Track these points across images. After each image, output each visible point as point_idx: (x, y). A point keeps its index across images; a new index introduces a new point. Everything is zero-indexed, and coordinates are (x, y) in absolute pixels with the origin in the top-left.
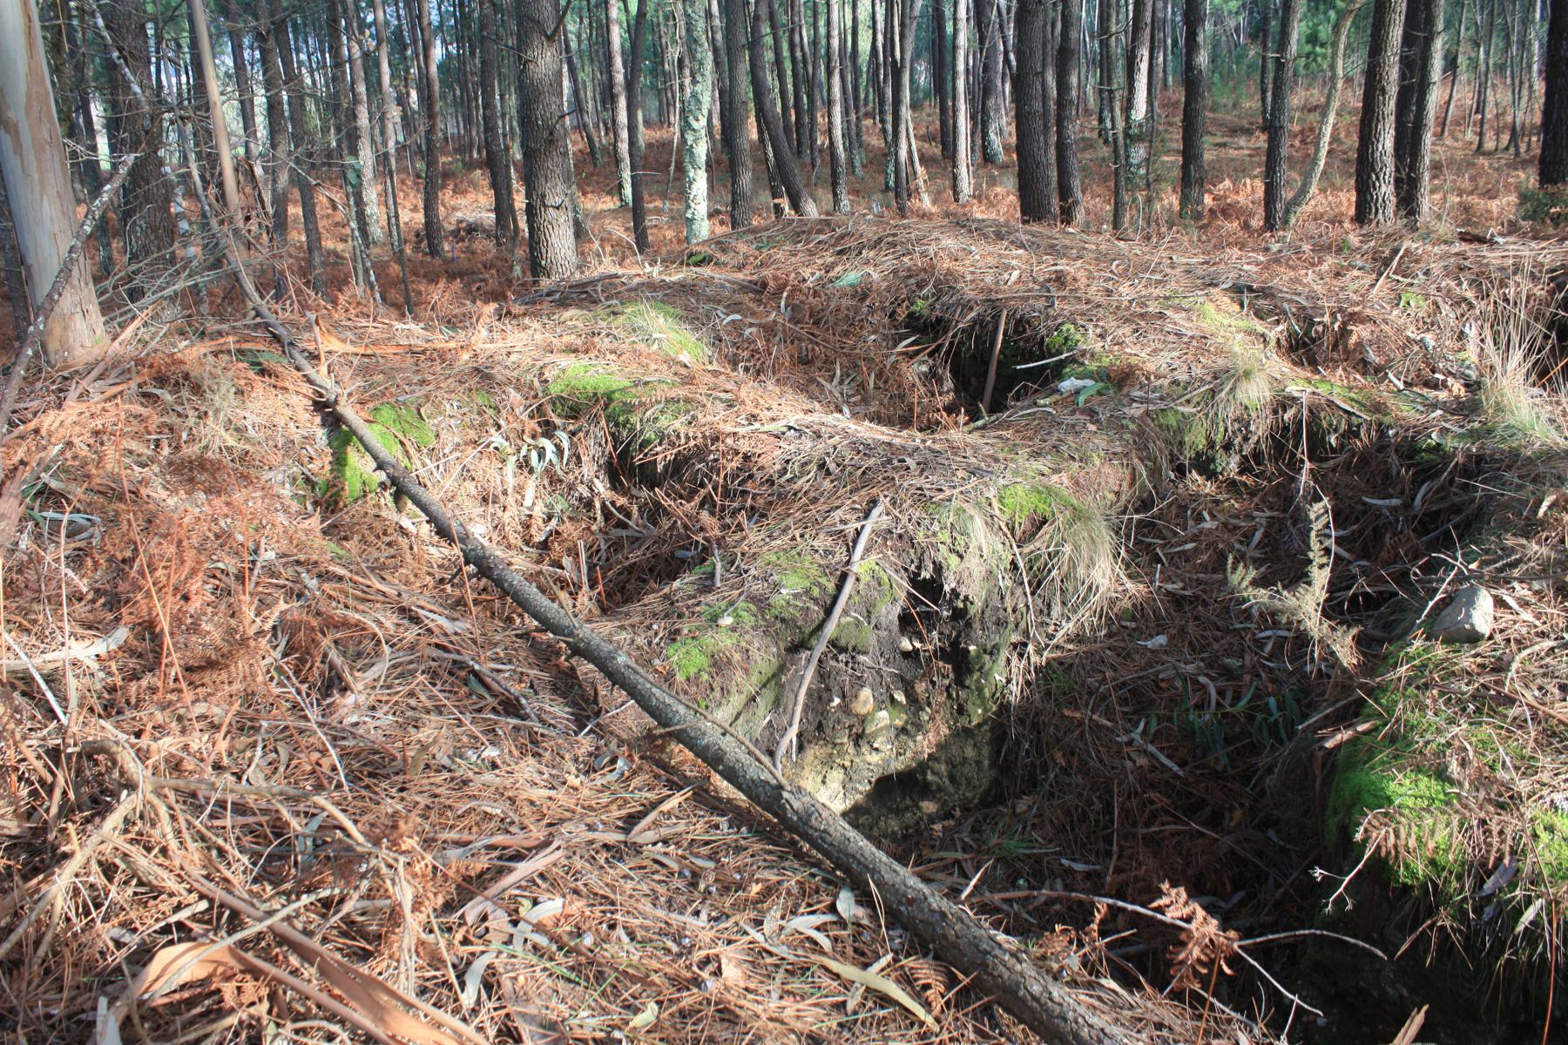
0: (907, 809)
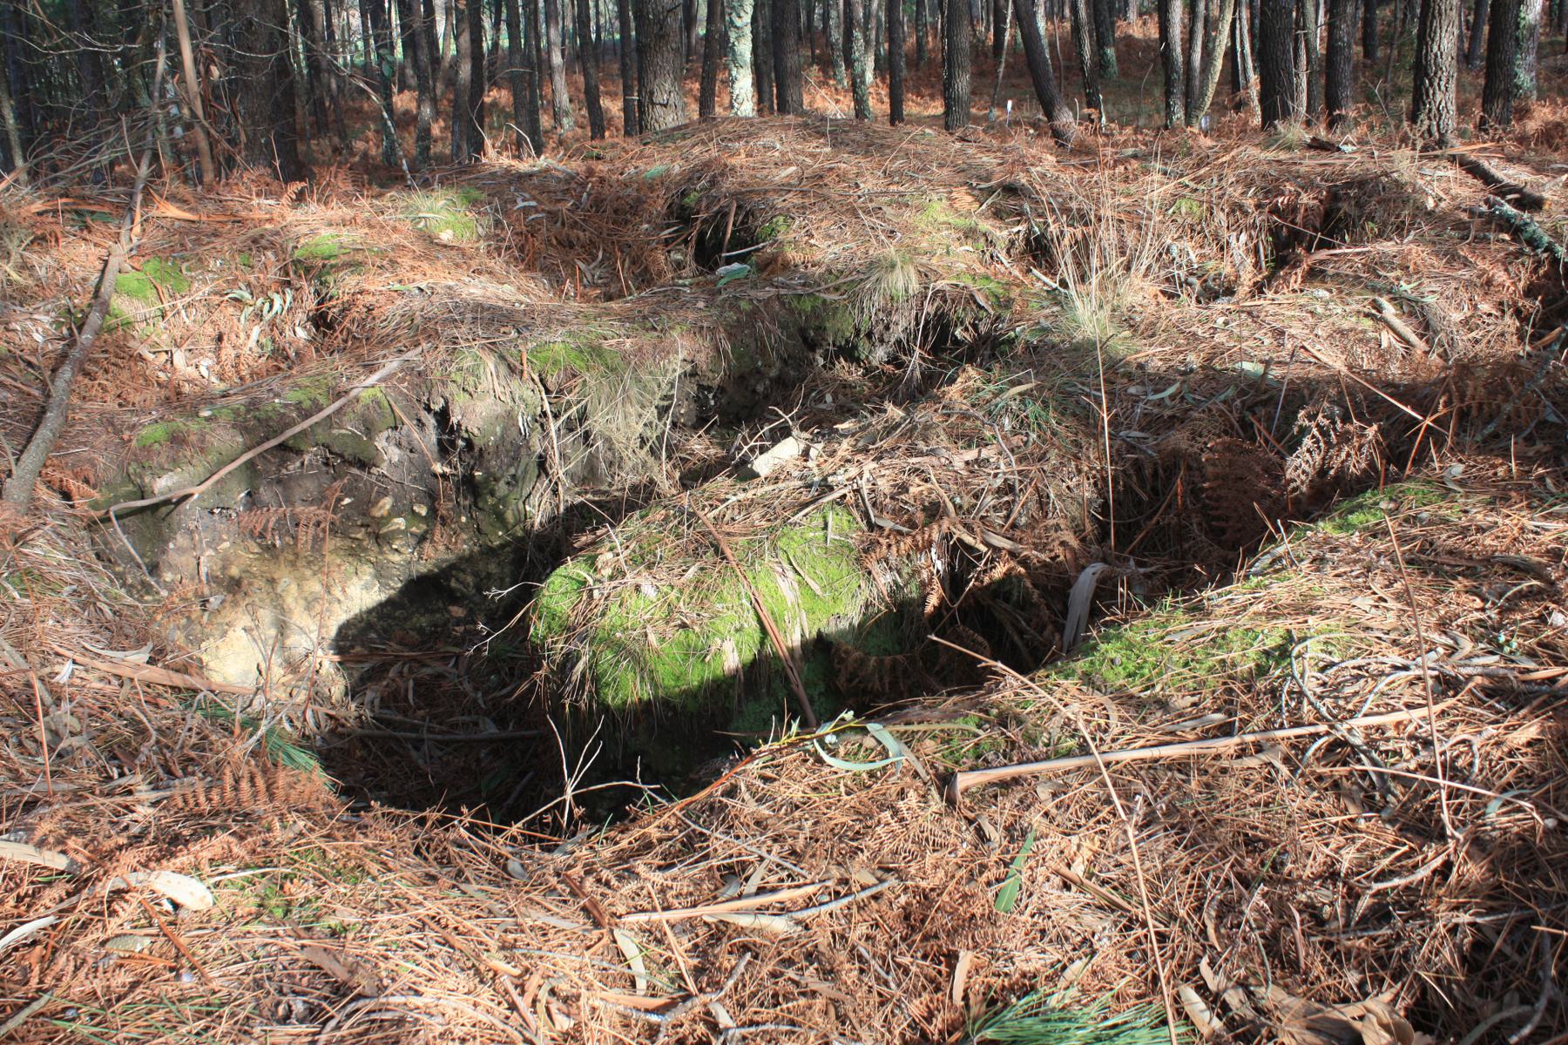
0: (438, 610)
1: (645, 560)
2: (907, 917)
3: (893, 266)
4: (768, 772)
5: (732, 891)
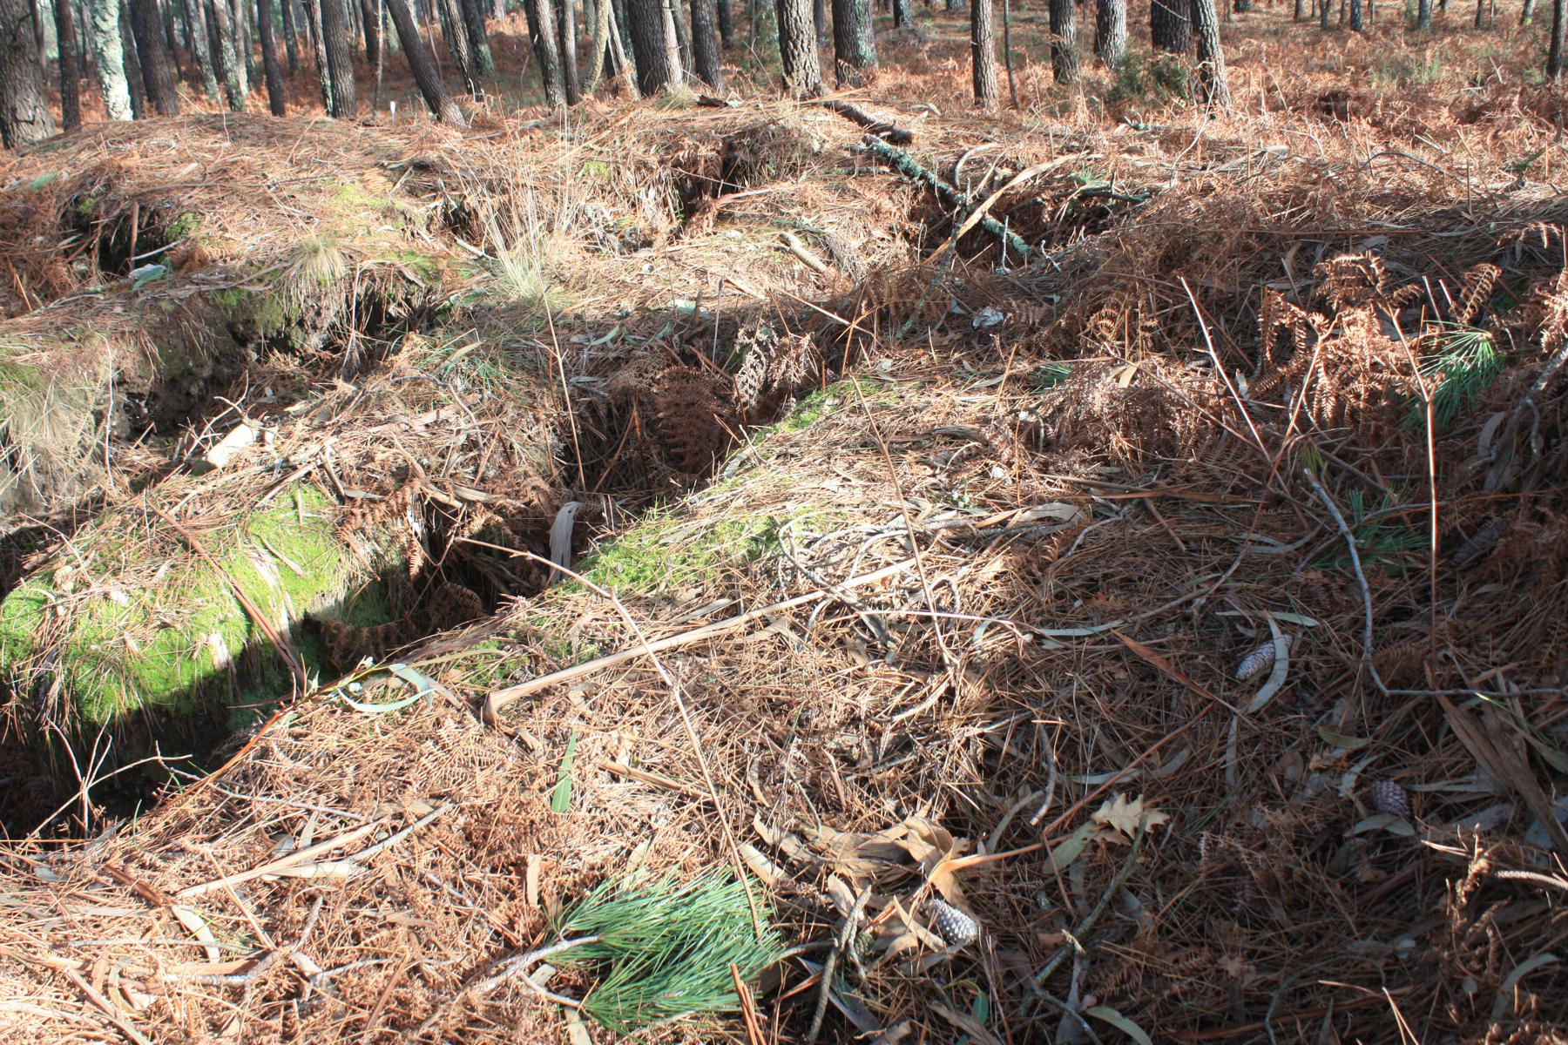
1: (109, 567)
2: (468, 838)
3: (316, 251)
4: (298, 730)
5: (288, 845)
